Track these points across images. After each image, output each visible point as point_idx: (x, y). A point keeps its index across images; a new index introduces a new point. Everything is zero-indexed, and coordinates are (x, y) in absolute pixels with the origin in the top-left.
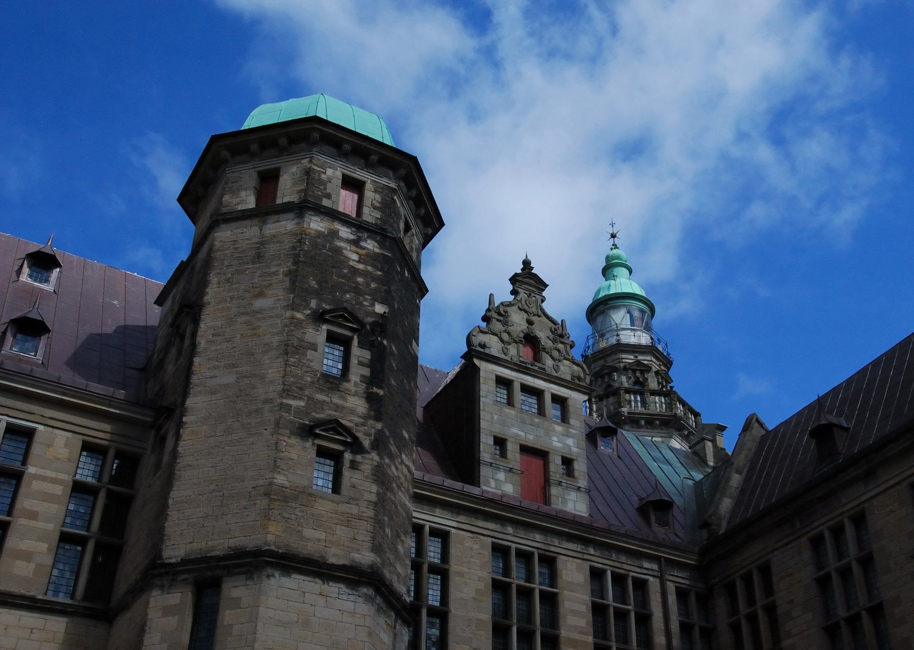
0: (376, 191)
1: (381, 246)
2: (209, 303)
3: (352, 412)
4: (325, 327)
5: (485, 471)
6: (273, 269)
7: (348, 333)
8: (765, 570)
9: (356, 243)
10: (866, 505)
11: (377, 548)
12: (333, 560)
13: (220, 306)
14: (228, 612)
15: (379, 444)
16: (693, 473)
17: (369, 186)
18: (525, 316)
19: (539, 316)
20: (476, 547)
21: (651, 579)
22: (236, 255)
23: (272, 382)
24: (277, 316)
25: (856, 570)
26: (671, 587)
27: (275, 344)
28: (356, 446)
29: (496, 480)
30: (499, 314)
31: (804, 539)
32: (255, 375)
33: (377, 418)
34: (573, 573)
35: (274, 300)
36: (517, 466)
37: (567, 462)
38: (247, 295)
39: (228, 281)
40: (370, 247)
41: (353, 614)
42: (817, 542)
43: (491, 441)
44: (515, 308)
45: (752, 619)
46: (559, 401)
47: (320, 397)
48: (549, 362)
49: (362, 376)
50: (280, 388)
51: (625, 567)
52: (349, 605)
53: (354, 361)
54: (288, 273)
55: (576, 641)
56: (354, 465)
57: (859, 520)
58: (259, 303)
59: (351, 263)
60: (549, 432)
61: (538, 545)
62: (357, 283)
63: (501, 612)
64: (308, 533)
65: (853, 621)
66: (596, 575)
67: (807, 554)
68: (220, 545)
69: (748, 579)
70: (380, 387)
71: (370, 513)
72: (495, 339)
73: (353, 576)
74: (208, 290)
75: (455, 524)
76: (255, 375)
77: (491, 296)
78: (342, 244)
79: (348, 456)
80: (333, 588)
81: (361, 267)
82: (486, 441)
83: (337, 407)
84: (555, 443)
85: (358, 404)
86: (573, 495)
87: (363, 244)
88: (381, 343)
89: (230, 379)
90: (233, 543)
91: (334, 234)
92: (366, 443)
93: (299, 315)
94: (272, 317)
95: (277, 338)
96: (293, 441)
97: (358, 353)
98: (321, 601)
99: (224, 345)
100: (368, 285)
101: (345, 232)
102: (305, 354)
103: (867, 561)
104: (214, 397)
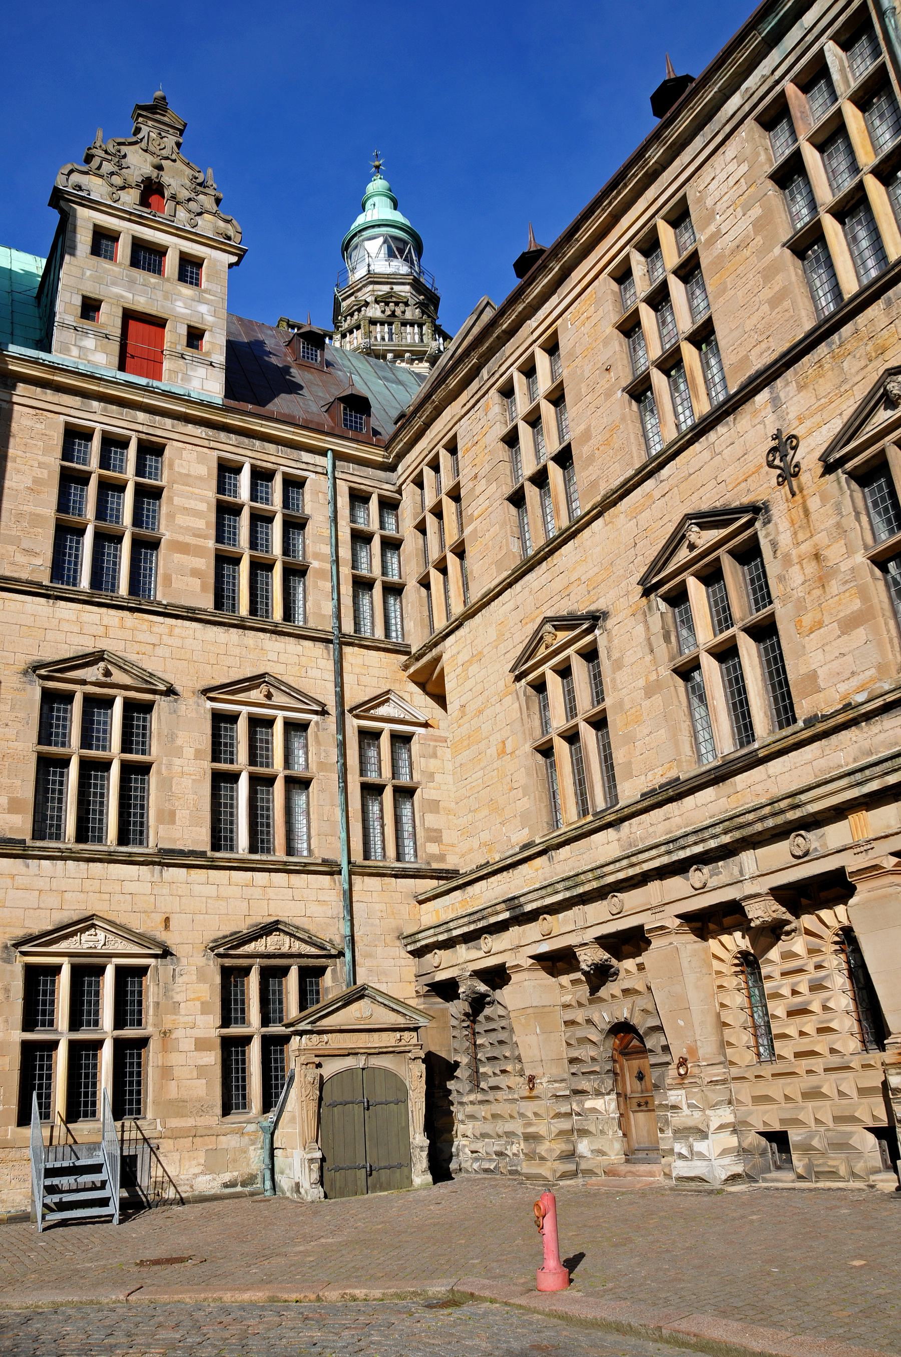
26: (343, 489)
51: (273, 459)
55: (187, 544)
61: (140, 428)
84: (178, 309)
86: (202, 371)
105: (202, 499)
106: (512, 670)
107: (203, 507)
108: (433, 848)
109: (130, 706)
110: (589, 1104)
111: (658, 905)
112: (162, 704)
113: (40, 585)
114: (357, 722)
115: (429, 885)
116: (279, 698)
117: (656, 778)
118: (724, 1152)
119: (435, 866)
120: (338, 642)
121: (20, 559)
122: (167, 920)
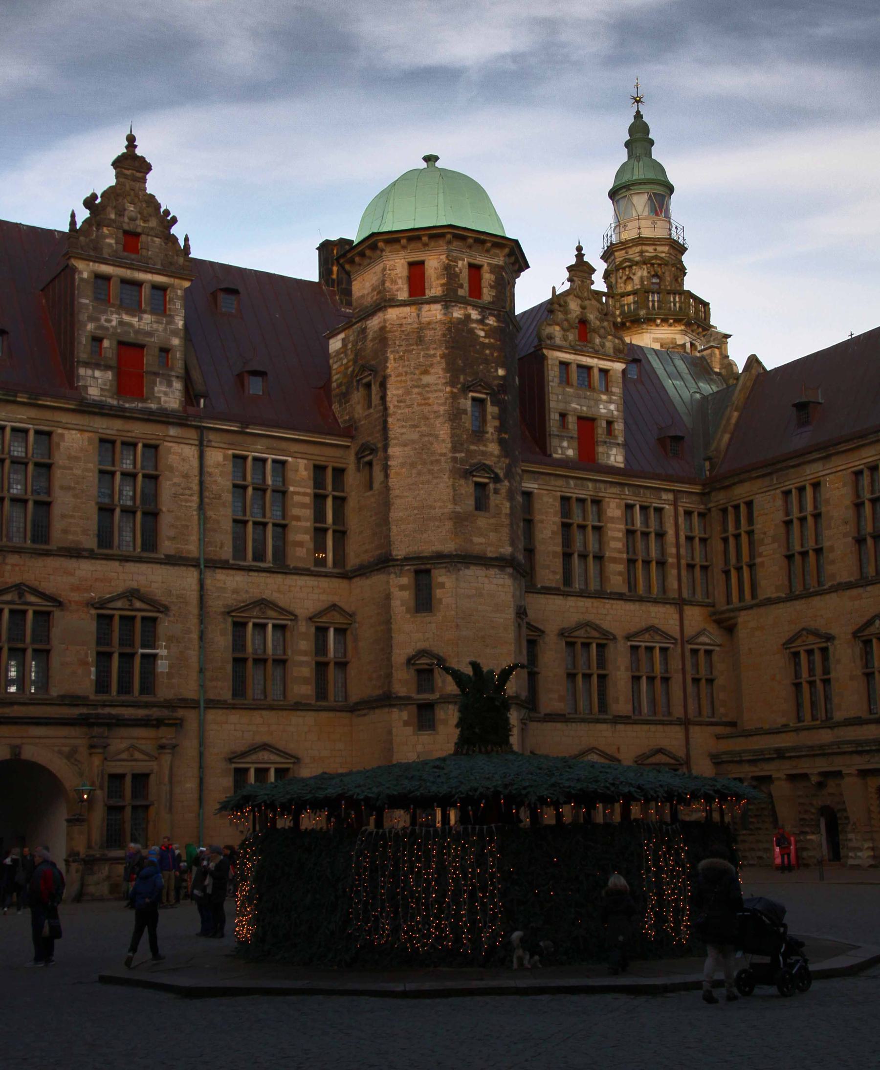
0: (491, 272)
1: (498, 321)
2: (390, 376)
3: (492, 454)
4: (471, 394)
5: (555, 442)
6: (432, 352)
7: (483, 396)
8: (749, 504)
9: (481, 322)
10: (822, 479)
11: (513, 544)
12: (489, 555)
13: (399, 379)
14: (438, 591)
15: (509, 474)
16: (701, 384)
17: (486, 268)
18: (579, 302)
19: (590, 299)
20: (551, 500)
21: (667, 507)
22: (403, 337)
23: (444, 441)
24: (440, 391)
25: (810, 520)
26: (681, 510)
27: (442, 413)
28: (496, 479)
29: (562, 448)
30: (560, 305)
31: (778, 491)
32: (431, 435)
33: (506, 457)
34: (613, 510)
35: (437, 376)
36: (575, 434)
37: (610, 423)
38: (417, 372)
39: (401, 358)
40: (491, 322)
41: (503, 586)
42: (787, 493)
43: (557, 417)
44: (571, 297)
45: (737, 536)
46: (604, 372)
47: (473, 447)
48: (597, 340)
49: (495, 427)
50: (449, 445)
51: (649, 500)
52: (501, 581)
53: (489, 417)
54: (443, 356)
55: (615, 558)
56: (496, 492)
57: (816, 486)
58: (426, 379)
59: (481, 339)
60: (598, 401)
61: (591, 493)
62: (486, 355)
63: (567, 542)
64: (476, 540)
65: (804, 554)
66: (629, 507)
67: (779, 503)
68: (427, 549)
69: (737, 508)
70: (506, 433)
71: (507, 521)
72: (557, 328)
73: (501, 563)
74: (388, 364)
75: (536, 486)
76: (431, 435)
77: (554, 288)
78: (474, 325)
79: (492, 486)
80: (492, 572)
81: (487, 341)
82: (555, 416)
83: (484, 453)
85: (493, 448)
86: (614, 451)
87: (487, 321)
88: (504, 399)
89: (415, 436)
90: (434, 548)
91: (468, 317)
92: (501, 475)
93: (455, 390)
94: (436, 391)
95: (442, 409)
96: (462, 482)
97: (491, 410)
98: (486, 581)
99: (406, 410)
100: (492, 354)
101: (475, 315)
102: (461, 419)
103: (817, 516)
104: (406, 449)
105: (619, 530)
106: (784, 644)
107: (620, 535)
108: (722, 710)
109: (599, 646)
110: (809, 837)
111: (851, 765)
112: (611, 645)
113: (558, 589)
114: (690, 646)
115: (719, 730)
116: (658, 638)
117: (852, 714)
118: (869, 857)
119: (724, 719)
120: (680, 603)
121: (551, 577)
122: (618, 749)
